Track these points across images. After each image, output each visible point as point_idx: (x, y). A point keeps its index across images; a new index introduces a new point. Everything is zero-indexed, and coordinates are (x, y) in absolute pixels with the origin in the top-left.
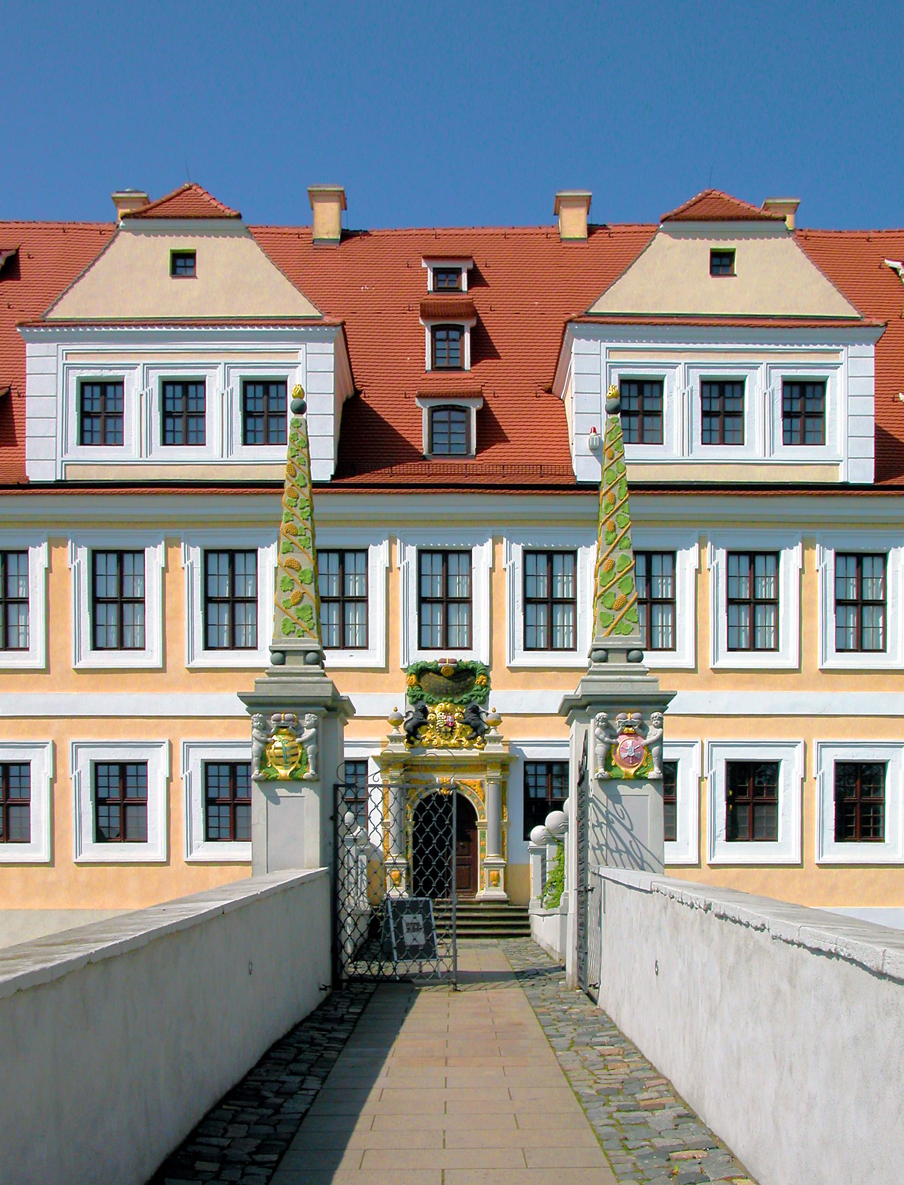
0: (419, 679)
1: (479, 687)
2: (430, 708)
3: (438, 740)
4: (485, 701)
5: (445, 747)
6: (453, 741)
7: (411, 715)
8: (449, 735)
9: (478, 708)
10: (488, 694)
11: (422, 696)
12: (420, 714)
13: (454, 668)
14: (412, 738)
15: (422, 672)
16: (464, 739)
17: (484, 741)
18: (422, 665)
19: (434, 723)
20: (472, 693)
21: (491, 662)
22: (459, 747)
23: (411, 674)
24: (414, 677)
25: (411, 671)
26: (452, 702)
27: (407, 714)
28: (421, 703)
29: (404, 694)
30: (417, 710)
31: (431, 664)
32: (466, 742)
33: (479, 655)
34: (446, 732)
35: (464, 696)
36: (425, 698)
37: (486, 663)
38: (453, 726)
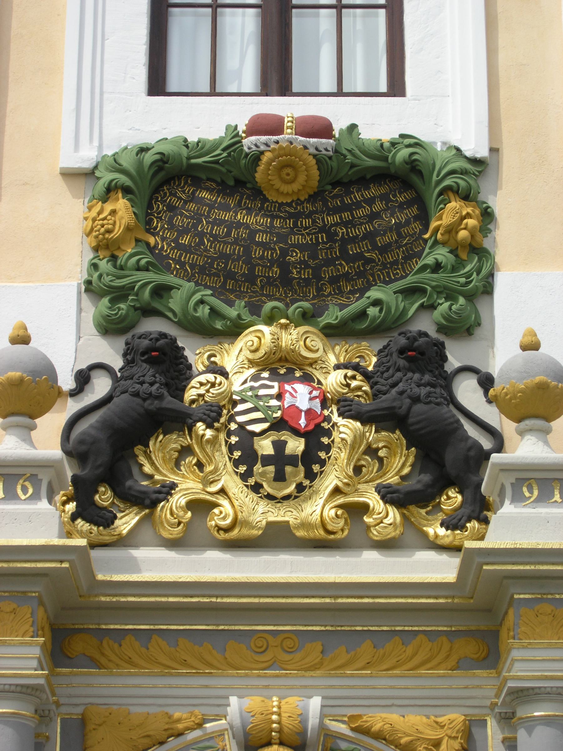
0: (146, 219)
1: (441, 254)
2: (197, 355)
3: (240, 504)
4: (465, 327)
5: (276, 538)
6: (318, 508)
7: (101, 386)
8: (296, 475)
9: (441, 346)
10: (488, 289)
11: (161, 291)
12: (146, 371)
13: (320, 160)
14: (104, 497)
15: (161, 182)
16: (373, 500)
17: (479, 509)
18: (165, 148)
19: (213, 414)
20: (410, 280)
21: (494, 150)
22: (350, 531)
23: (110, 191)
24: (121, 204)
25: (107, 177)
26: (306, 318)
27: (83, 379)
28: (153, 326)
29: (75, 283)
30: (130, 355)
31: (201, 147)
32: (385, 517)
33: (440, 112)
34: (280, 460)
35: (374, 293)
36: (175, 302)
37: (475, 146)
38: (317, 437)
